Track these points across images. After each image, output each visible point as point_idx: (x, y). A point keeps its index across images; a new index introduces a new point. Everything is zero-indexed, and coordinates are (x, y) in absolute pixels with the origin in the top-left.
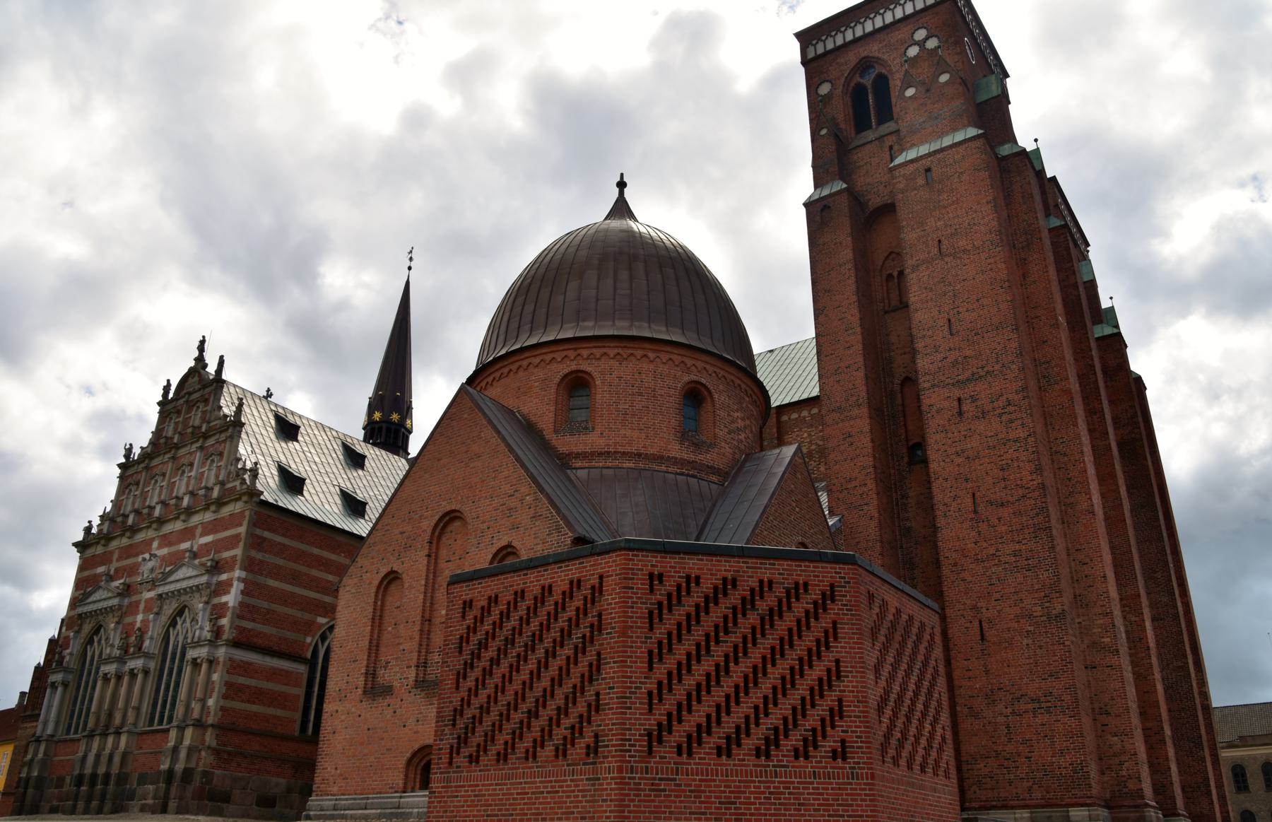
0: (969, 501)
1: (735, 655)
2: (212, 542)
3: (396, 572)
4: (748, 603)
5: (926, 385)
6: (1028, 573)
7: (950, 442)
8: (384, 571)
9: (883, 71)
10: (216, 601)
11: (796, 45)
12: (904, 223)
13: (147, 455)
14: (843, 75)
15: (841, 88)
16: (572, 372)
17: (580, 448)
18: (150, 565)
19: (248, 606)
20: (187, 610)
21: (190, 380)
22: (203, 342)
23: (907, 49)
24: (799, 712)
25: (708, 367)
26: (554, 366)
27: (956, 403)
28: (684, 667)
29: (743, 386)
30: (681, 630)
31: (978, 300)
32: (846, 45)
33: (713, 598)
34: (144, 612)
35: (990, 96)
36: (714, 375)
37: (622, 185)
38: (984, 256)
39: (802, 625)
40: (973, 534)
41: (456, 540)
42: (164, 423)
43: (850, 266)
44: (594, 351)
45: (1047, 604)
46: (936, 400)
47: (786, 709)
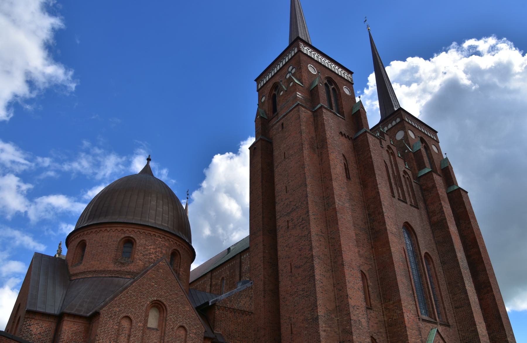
6: (307, 299)
12: (275, 148)
27: (287, 223)
31: (295, 176)
36: (138, 232)
45: (312, 313)
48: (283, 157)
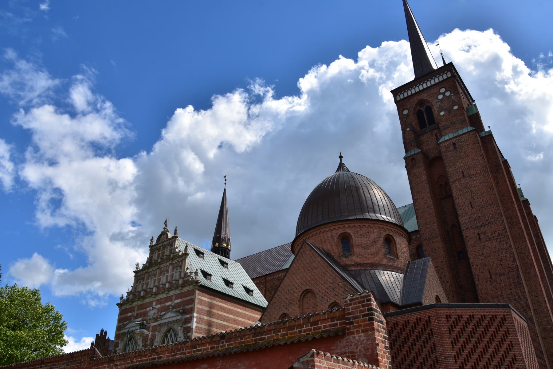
0: (488, 274)
2: (181, 302)
3: (286, 314)
4: (479, 324)
5: (464, 228)
6: (515, 302)
7: (477, 251)
8: (280, 313)
9: (429, 105)
10: (185, 326)
11: (391, 95)
12: (447, 165)
13: (145, 267)
14: (412, 107)
15: (412, 111)
16: (342, 233)
17: (350, 263)
18: (153, 312)
19: (198, 327)
20: (171, 330)
21: (163, 237)
22: (166, 222)
23: (438, 96)
25: (391, 228)
26: (335, 231)
27: (477, 235)
28: (464, 346)
29: (403, 235)
32: (412, 95)
33: (468, 322)
34: (152, 331)
35: (474, 113)
37: (341, 157)
38: (481, 177)
39: (497, 330)
40: (491, 287)
41: (310, 301)
42: (153, 254)
44: (350, 225)
46: (469, 234)
47: (498, 359)
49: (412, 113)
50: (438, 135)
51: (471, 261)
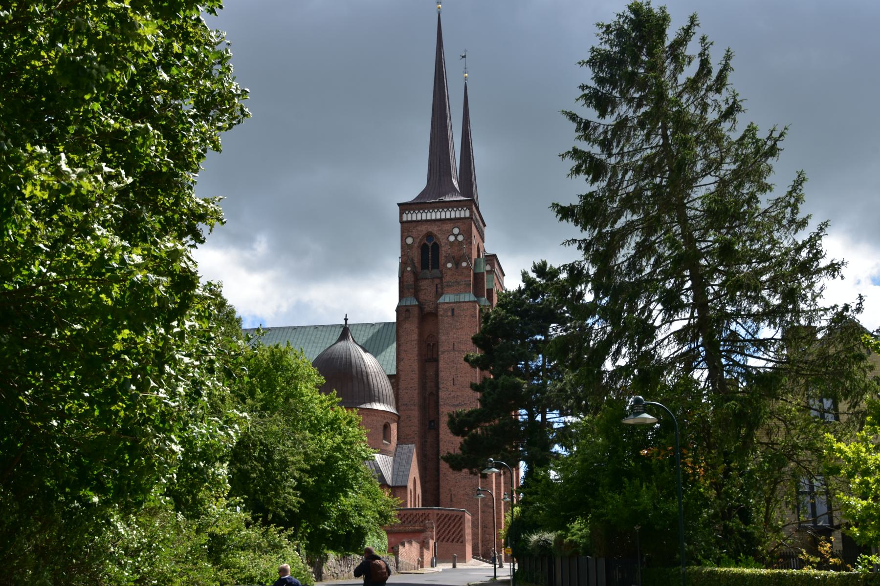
1: (449, 526)
4: (450, 519)
24: (457, 536)
28: (442, 529)
30: (441, 522)
32: (421, 221)
33: (445, 518)
39: (457, 522)
43: (415, 342)
48: (452, 347)
49: (416, 245)
50: (439, 286)
51: (441, 436)
